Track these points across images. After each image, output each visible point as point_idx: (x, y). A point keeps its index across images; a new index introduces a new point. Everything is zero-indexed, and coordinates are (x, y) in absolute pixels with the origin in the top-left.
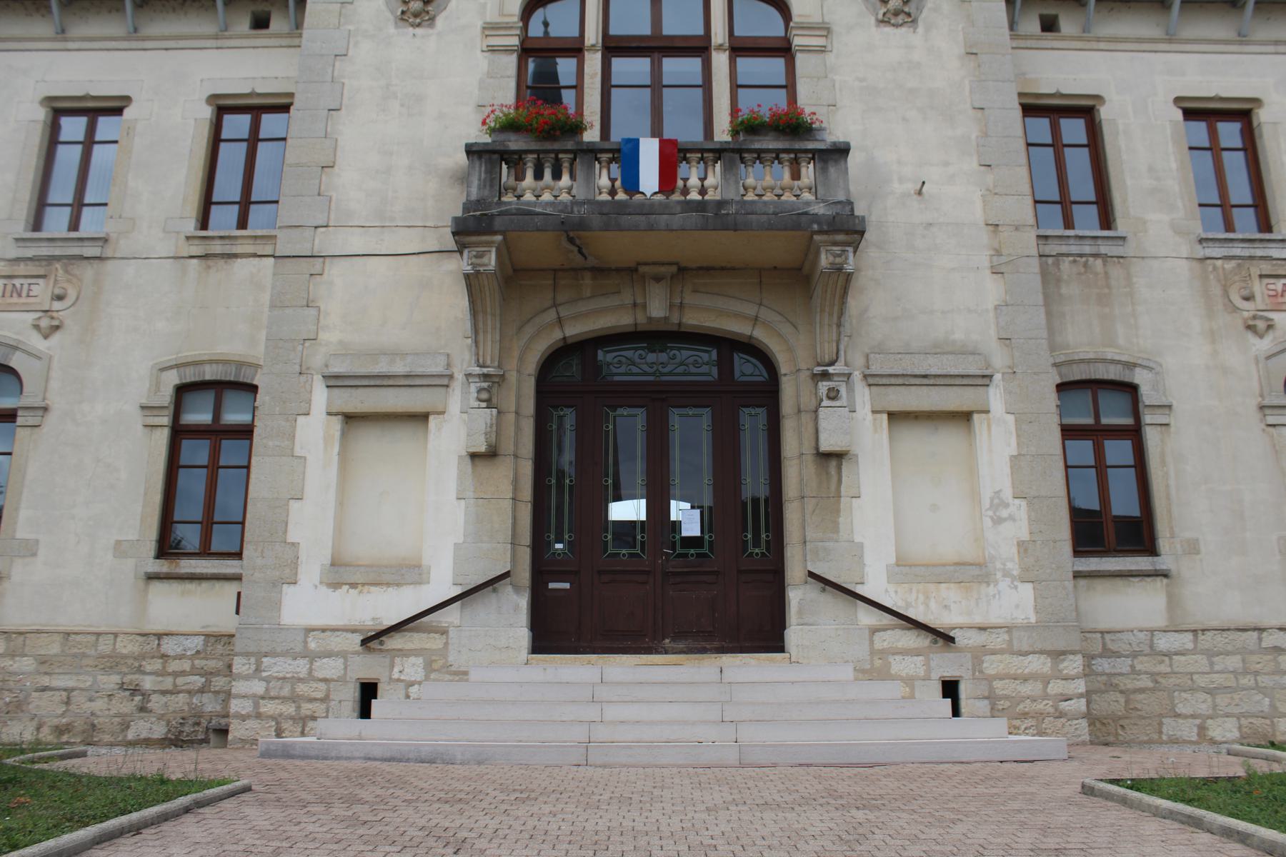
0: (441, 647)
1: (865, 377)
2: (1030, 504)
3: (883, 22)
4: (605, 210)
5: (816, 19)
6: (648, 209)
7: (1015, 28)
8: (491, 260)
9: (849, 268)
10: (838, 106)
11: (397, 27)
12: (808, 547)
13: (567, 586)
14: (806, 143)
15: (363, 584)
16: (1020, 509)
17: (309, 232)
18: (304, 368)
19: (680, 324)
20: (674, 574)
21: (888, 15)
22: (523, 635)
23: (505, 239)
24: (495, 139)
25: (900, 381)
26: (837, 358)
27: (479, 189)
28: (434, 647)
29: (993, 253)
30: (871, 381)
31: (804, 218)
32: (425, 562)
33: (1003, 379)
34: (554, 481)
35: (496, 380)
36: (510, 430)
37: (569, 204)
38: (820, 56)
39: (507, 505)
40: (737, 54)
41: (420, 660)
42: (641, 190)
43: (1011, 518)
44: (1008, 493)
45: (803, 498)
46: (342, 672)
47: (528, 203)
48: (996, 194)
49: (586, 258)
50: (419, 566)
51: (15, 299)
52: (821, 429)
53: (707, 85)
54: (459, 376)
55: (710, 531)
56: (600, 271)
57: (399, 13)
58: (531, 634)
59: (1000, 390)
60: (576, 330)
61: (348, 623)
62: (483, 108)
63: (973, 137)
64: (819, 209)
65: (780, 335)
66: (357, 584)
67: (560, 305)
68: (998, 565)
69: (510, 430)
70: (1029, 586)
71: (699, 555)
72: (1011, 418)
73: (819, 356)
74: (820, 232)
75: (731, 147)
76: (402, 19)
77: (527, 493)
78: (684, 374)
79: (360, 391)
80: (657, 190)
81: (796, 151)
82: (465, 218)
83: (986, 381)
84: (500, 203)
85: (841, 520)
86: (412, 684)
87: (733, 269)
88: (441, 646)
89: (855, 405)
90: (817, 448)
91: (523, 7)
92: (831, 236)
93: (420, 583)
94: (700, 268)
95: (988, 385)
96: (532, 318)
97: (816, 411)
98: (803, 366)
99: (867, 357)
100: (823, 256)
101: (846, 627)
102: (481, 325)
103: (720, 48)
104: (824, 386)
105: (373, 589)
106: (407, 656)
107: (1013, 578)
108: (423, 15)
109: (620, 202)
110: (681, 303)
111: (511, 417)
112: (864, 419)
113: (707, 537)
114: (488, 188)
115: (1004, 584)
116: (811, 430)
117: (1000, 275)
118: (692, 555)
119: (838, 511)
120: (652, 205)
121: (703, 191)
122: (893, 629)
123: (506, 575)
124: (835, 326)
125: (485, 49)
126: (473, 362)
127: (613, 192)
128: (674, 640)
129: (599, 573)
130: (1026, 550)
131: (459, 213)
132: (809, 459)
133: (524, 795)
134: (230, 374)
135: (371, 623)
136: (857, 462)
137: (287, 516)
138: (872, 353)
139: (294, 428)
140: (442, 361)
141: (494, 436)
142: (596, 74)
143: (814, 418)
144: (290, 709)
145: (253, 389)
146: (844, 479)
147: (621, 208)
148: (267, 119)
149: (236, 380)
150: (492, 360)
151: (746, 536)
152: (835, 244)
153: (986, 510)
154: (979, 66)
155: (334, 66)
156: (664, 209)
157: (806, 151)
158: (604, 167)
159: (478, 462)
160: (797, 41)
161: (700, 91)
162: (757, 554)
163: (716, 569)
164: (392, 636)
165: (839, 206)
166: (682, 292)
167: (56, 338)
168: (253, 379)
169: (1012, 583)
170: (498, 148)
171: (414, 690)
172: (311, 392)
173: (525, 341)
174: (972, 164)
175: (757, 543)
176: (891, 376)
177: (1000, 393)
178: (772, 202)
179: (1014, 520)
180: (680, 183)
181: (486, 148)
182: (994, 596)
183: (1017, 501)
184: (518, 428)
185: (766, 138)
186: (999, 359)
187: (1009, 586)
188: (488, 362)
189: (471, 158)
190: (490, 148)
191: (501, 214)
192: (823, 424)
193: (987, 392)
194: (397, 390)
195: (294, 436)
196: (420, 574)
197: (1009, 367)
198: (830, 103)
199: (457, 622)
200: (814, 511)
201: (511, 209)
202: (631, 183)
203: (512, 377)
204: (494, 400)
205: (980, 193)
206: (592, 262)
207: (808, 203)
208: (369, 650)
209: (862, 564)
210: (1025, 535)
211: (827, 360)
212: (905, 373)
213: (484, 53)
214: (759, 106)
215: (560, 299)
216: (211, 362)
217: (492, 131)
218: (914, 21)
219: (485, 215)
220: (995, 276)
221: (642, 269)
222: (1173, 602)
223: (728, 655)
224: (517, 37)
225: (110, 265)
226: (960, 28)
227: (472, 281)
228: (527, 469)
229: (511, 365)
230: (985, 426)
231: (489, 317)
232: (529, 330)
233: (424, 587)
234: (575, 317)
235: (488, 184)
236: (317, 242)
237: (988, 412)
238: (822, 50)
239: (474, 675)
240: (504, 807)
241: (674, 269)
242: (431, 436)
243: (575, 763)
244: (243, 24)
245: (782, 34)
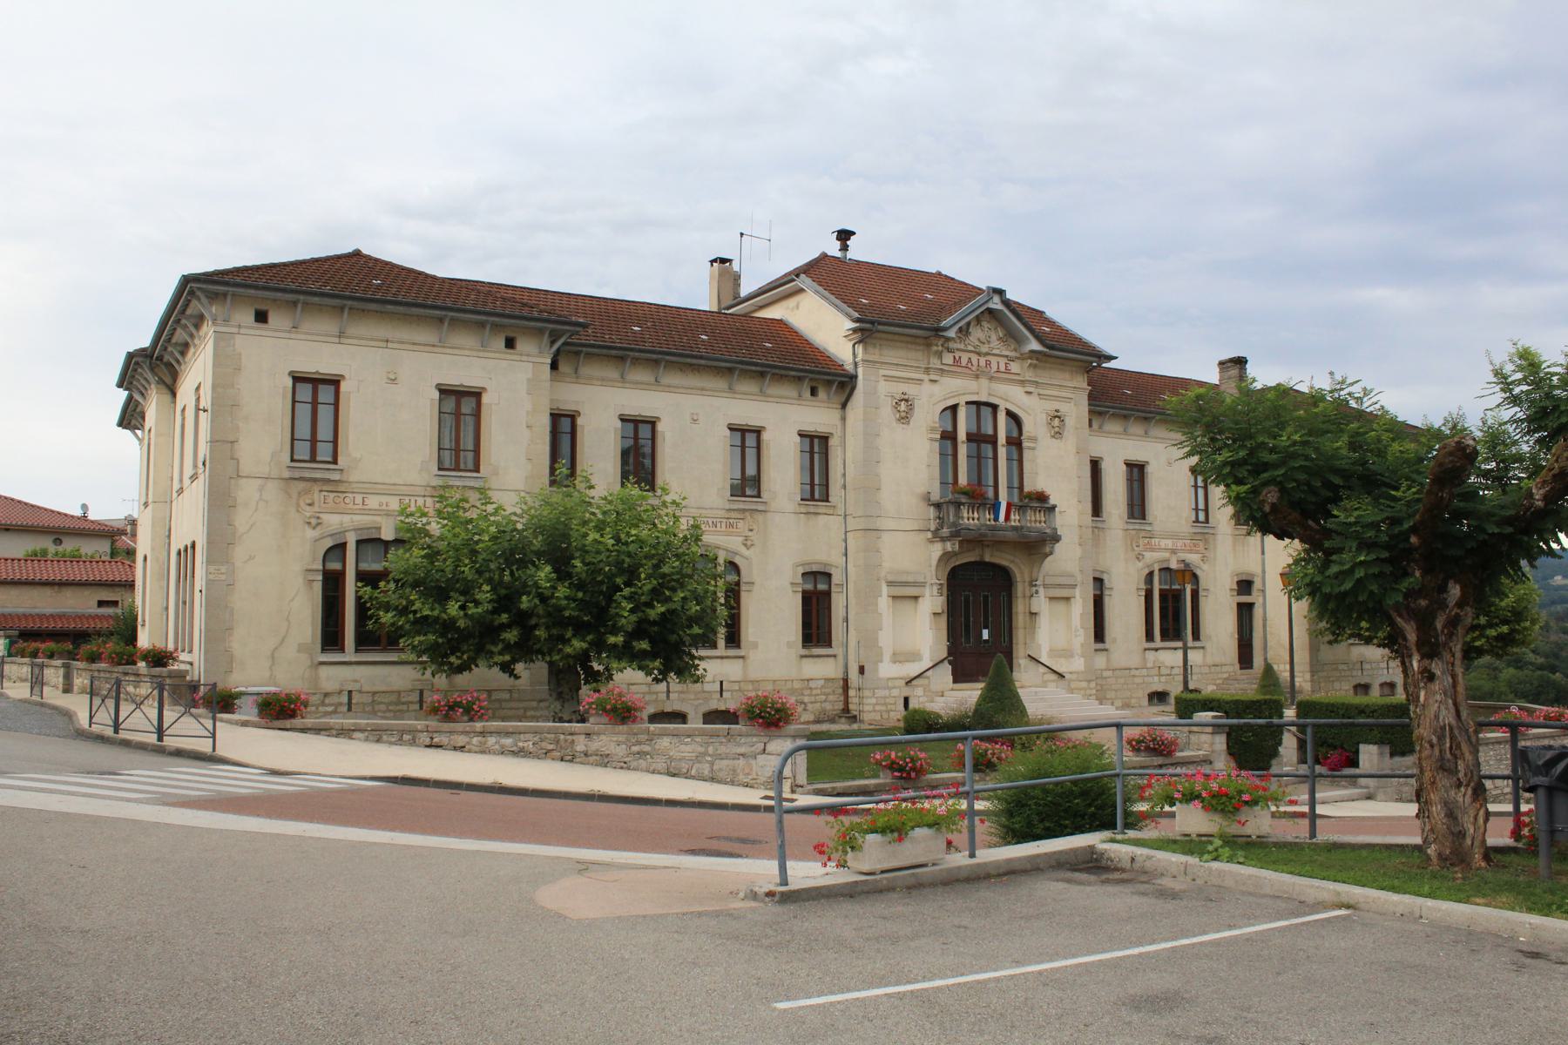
3: (1053, 437)
51: (731, 529)
144: (884, 708)
167: (752, 549)
222: (1108, 660)
225: (769, 514)
238: (1034, 449)
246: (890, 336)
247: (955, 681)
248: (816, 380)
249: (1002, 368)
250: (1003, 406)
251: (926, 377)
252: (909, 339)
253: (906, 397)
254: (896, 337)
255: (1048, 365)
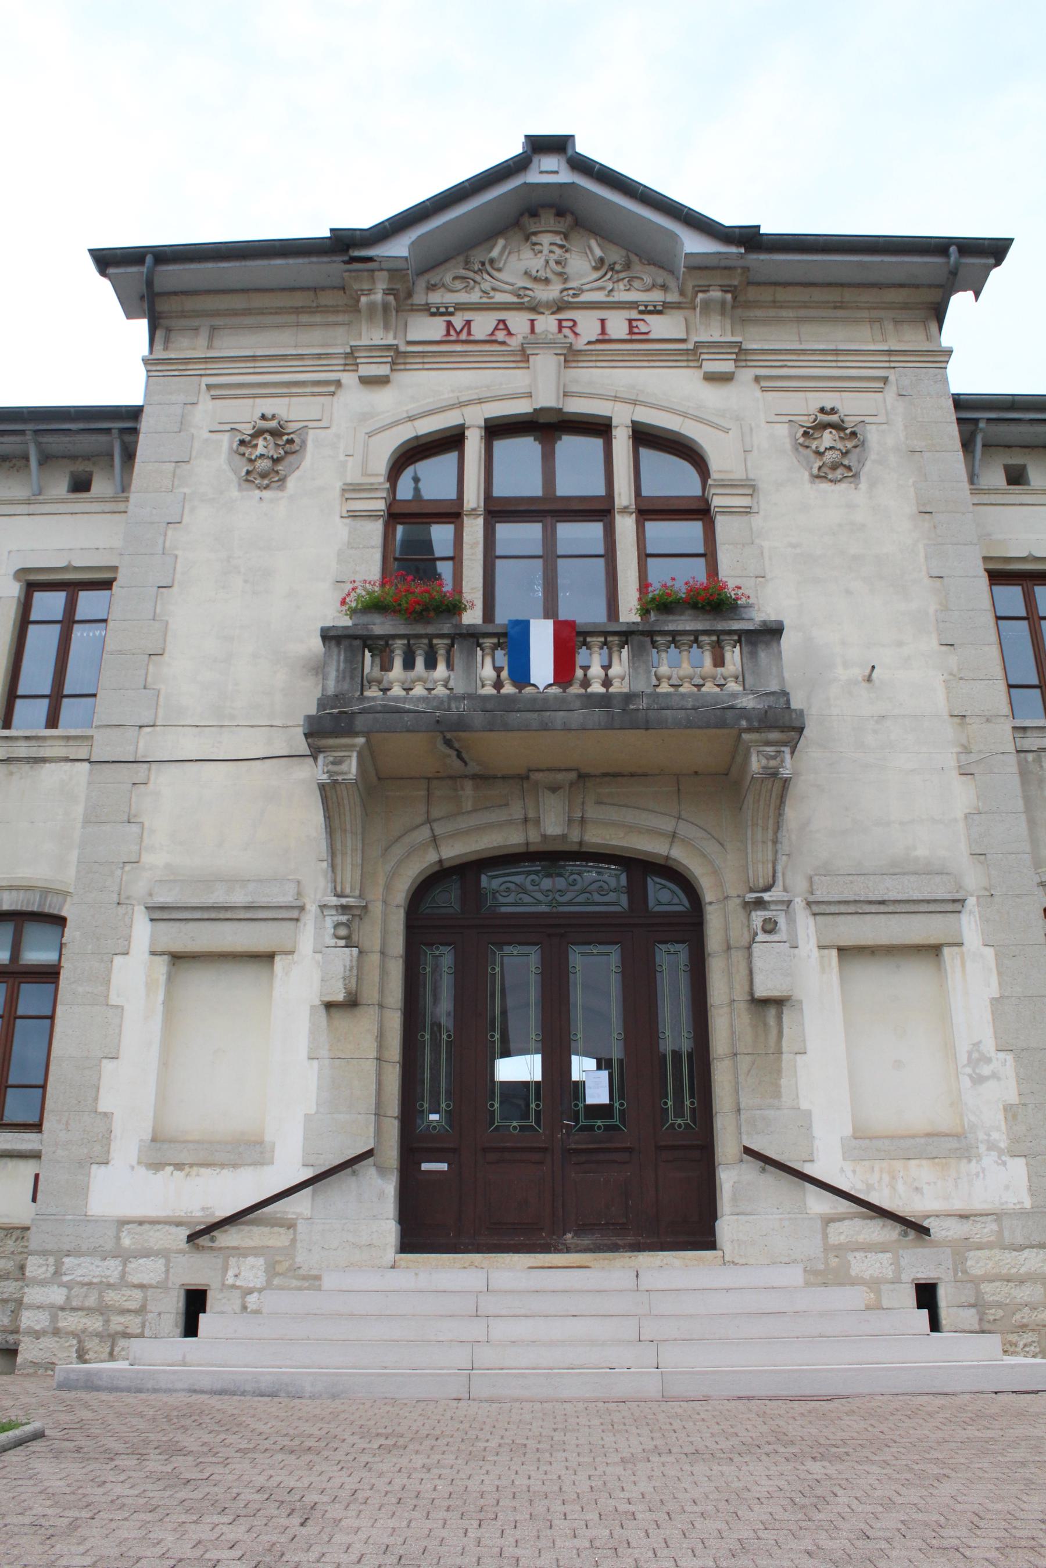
0: (287, 1244)
1: (809, 904)
2: (1017, 1059)
3: (819, 477)
4: (489, 706)
5: (739, 474)
6: (541, 705)
7: (976, 481)
8: (351, 768)
9: (785, 772)
10: (768, 577)
11: (240, 489)
12: (743, 1117)
13: (444, 1167)
14: (731, 622)
15: (191, 1165)
16: (1005, 1065)
17: (132, 733)
18: (123, 896)
19: (581, 843)
20: (577, 1151)
21: (825, 469)
22: (389, 1230)
23: (368, 741)
24: (357, 622)
25: (852, 909)
26: (774, 882)
27: (337, 681)
28: (279, 1244)
29: (959, 750)
30: (816, 909)
31: (729, 714)
32: (268, 1138)
33: (978, 904)
34: (427, 1037)
35: (357, 912)
36: (373, 976)
37: (445, 699)
38: (745, 518)
39: (371, 1066)
40: (646, 517)
41: (260, 1261)
42: (532, 682)
43: (995, 1076)
44: (989, 1045)
45: (735, 1055)
46: (163, 1276)
47: (396, 699)
48: (961, 679)
49: (466, 764)
50: (261, 1143)
52: (755, 970)
53: (610, 555)
54: (312, 908)
55: (621, 1097)
56: (483, 779)
57: (243, 473)
58: (399, 1227)
59: (975, 916)
60: (454, 851)
61: (171, 1214)
62: (342, 584)
63: (931, 610)
64: (748, 702)
65: (704, 856)
66: (184, 1164)
67: (435, 820)
68: (981, 1136)
69: (373, 976)
70: (1022, 1161)
71: (607, 1128)
72: (989, 952)
73: (751, 881)
74: (749, 730)
75: (640, 629)
76: (247, 480)
77: (394, 1050)
78: (587, 903)
79: (191, 925)
80: (552, 682)
81: (719, 633)
82: (320, 717)
83: (957, 907)
84: (362, 698)
85: (783, 1082)
86: (250, 1291)
87: (645, 775)
88: (287, 1244)
89: (797, 939)
90: (751, 993)
91: (392, 463)
92: (763, 734)
93: (262, 1164)
94: (605, 775)
95: (959, 912)
96: (400, 837)
97: (749, 948)
98: (732, 893)
99: (810, 879)
100: (754, 759)
101: (793, 1216)
102: (338, 846)
103: (625, 510)
104: (758, 917)
105: (203, 1170)
106: (245, 1256)
107: (1001, 1152)
108: (272, 475)
109: (507, 696)
110: (582, 817)
111: (375, 958)
112: (809, 957)
113: (617, 1104)
114: (348, 679)
115: (989, 1160)
116: (744, 972)
117: (969, 776)
118: (599, 1128)
119: (779, 1071)
120: (546, 700)
121: (607, 682)
122: (851, 1219)
123: (369, 1154)
124: (770, 844)
125: (345, 514)
126: (329, 890)
127: (498, 685)
128: (577, 1234)
129: (485, 1150)
130: (1015, 1117)
131: (313, 711)
132: (742, 1007)
133: (390, 1442)
134: (33, 904)
135: (200, 1214)
136: (801, 1010)
137: (99, 1079)
138: (816, 875)
139: (109, 971)
140: (291, 889)
141: (354, 981)
142: (477, 543)
143: (746, 956)
144: (95, 1324)
145: (60, 921)
146: (786, 1031)
147: (508, 704)
148: (85, 598)
149: (40, 910)
150: (352, 889)
151: (666, 1103)
152: (768, 743)
153: (964, 1066)
154: (935, 527)
155: (165, 535)
156: (561, 705)
157: (730, 632)
158: (488, 654)
159: (336, 1014)
160: (716, 502)
161: (601, 562)
162: (680, 1126)
163: (628, 1145)
164: (226, 1231)
165: (772, 698)
166: (583, 803)
168: (61, 909)
169: (999, 1157)
170: (360, 632)
171: (252, 1300)
172: (131, 927)
173: (393, 864)
174: (930, 643)
175: (679, 1112)
176: (839, 902)
177: (976, 922)
178: (691, 695)
179: (999, 1079)
180: (579, 673)
181: (346, 632)
182: (977, 1175)
183: (1001, 1055)
184: (384, 971)
185: (683, 618)
186: (972, 879)
187: (996, 1162)
188: (348, 891)
189: (327, 643)
190: (351, 632)
191: (363, 711)
192: (758, 963)
193: (960, 919)
194: (236, 924)
195: (109, 981)
196: (262, 1153)
197: (986, 889)
198: (758, 574)
199: (307, 1213)
200: (749, 1071)
201: (376, 706)
202: (521, 673)
203: (377, 909)
204: (355, 937)
205: (942, 678)
206: (473, 768)
207: (734, 695)
208: (198, 1248)
209: (811, 1138)
210: (1013, 1098)
211: (761, 883)
212: (857, 899)
213: (343, 520)
214: (673, 579)
215: (435, 813)
216: (10, 888)
217: (353, 612)
218: (856, 476)
219: (345, 713)
220: (964, 778)
221: (535, 776)
223: (645, 1253)
224: (384, 501)
226: (911, 481)
227: (328, 793)
228: (395, 1021)
229: (376, 894)
230: (958, 962)
231: (349, 835)
232: (398, 851)
233: (267, 1169)
234: (455, 835)
235: (348, 675)
236: (141, 745)
237: (960, 944)
238: (747, 511)
239: (329, 1281)
240: (364, 1458)
241: (573, 775)
242: (277, 982)
243: (454, 1396)
244: (60, 487)
245: (698, 493)
246: (238, 302)
247: (406, 1247)
248: (87, 458)
249: (617, 326)
250: (622, 419)
251: (349, 379)
252: (299, 300)
253: (273, 424)
254: (259, 301)
255: (790, 313)
